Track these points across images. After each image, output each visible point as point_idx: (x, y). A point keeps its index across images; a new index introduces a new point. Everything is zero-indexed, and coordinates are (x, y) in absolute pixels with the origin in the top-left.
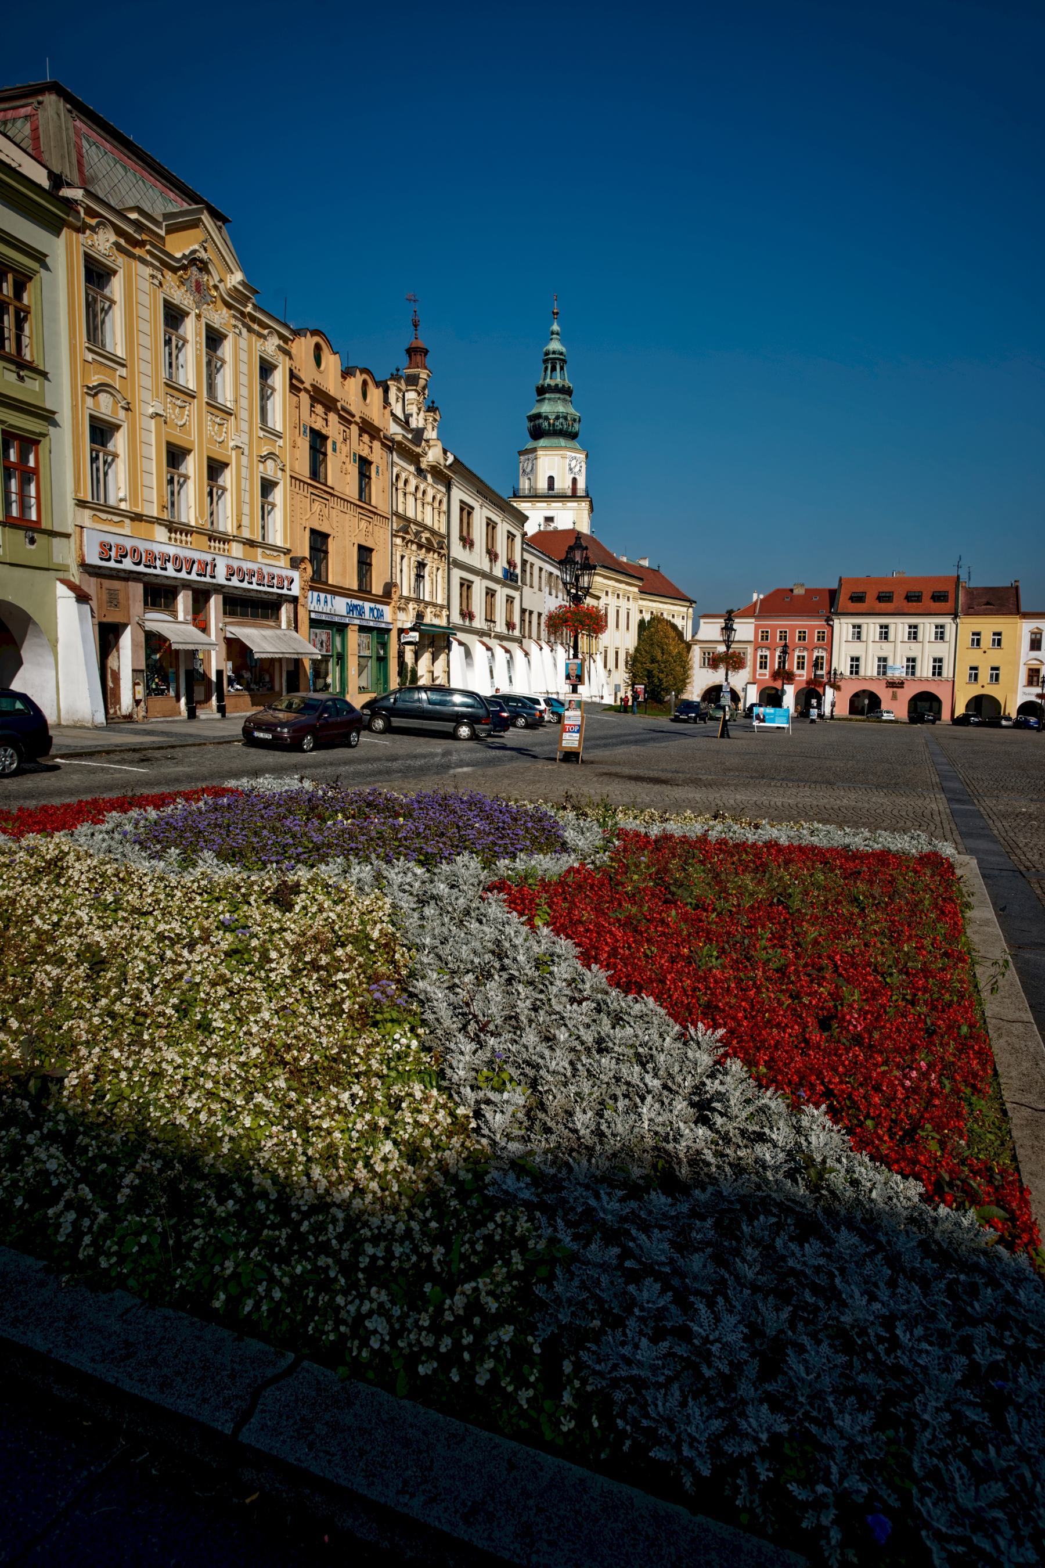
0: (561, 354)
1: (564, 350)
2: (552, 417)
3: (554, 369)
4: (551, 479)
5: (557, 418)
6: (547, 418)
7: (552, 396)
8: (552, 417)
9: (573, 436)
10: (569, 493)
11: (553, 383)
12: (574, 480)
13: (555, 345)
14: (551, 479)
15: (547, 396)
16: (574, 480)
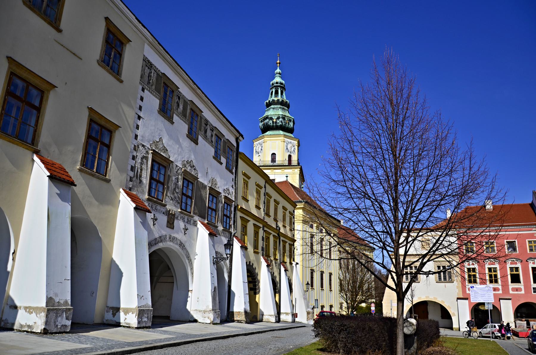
0: (282, 84)
1: (283, 82)
2: (275, 118)
3: (277, 93)
4: (274, 155)
5: (278, 118)
6: (271, 119)
7: (276, 106)
8: (275, 118)
9: (291, 131)
10: (286, 163)
11: (276, 99)
12: (290, 156)
13: (278, 79)
14: (274, 155)
15: (272, 106)
16: (290, 156)
